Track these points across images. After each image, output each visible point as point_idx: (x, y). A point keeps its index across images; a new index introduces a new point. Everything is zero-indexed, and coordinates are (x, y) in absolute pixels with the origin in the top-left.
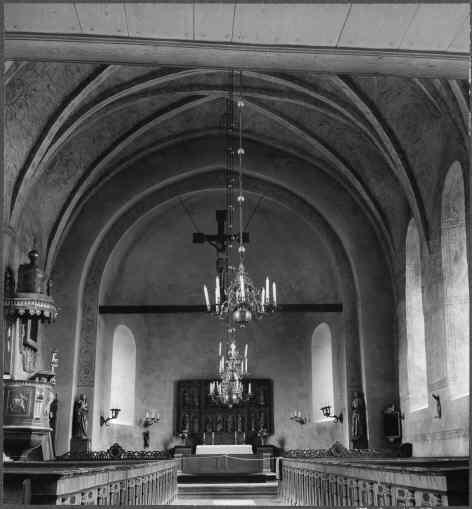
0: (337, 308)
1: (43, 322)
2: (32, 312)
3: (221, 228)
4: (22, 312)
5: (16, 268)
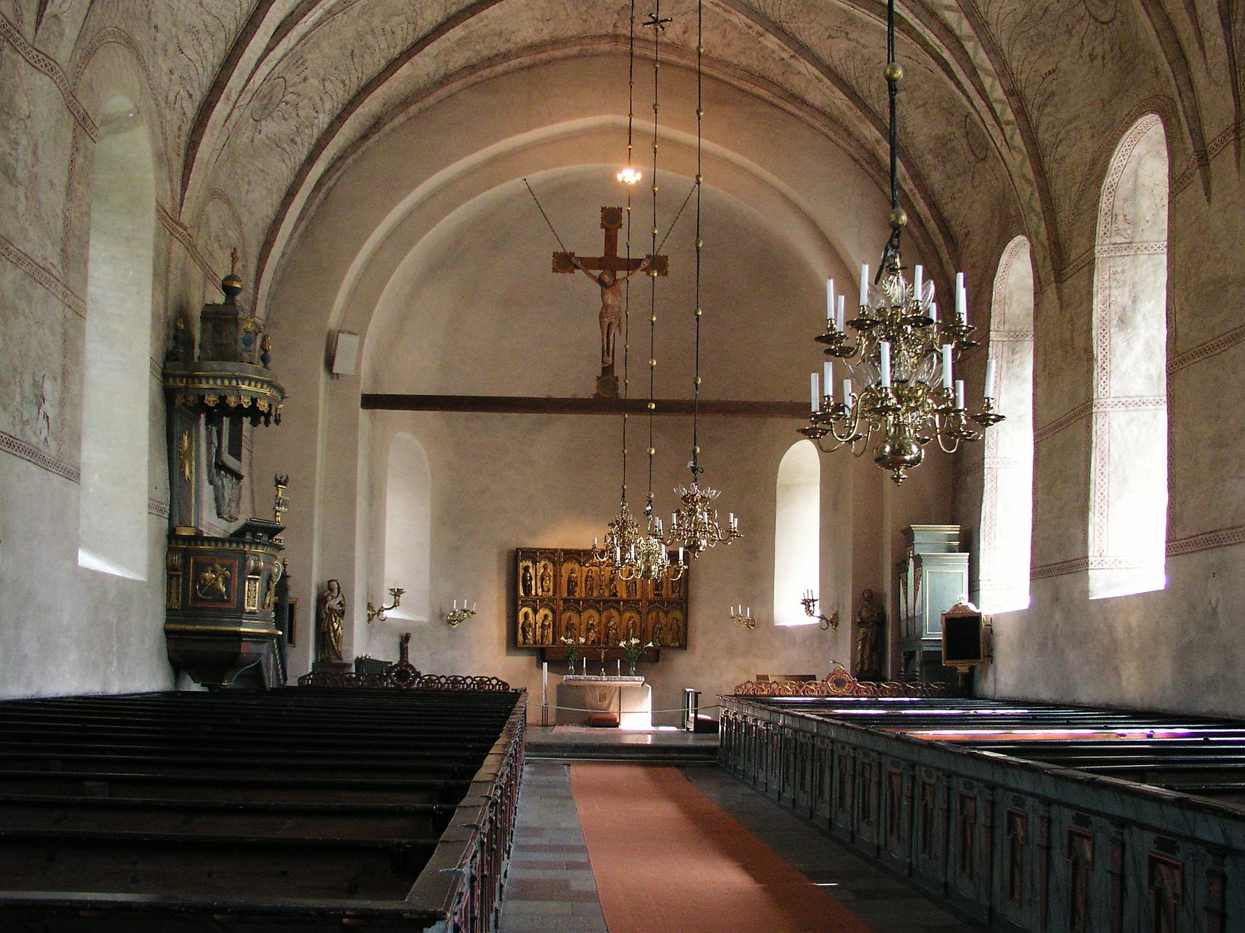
1: (255, 423)
2: (232, 401)
3: (611, 242)
4: (211, 400)
5: (197, 312)
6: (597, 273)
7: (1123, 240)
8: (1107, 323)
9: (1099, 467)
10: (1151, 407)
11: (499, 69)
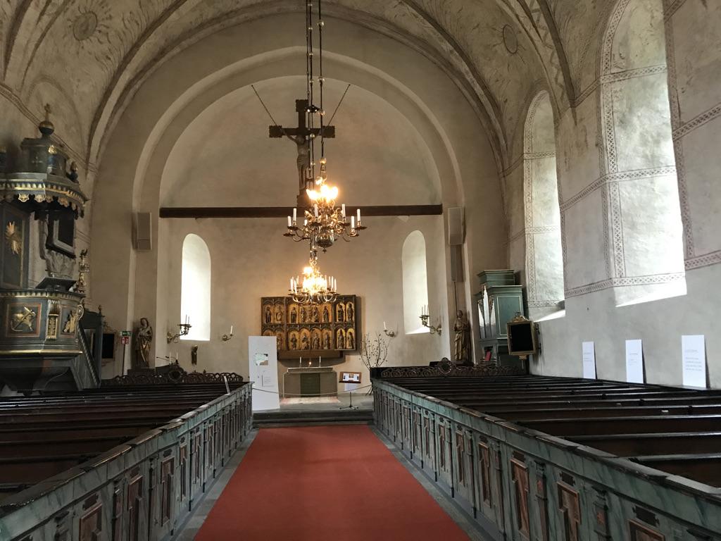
0: (435, 210)
3: (302, 119)
6: (294, 137)
7: (620, 70)
8: (612, 125)
9: (614, 218)
10: (648, 176)
11: (234, 20)
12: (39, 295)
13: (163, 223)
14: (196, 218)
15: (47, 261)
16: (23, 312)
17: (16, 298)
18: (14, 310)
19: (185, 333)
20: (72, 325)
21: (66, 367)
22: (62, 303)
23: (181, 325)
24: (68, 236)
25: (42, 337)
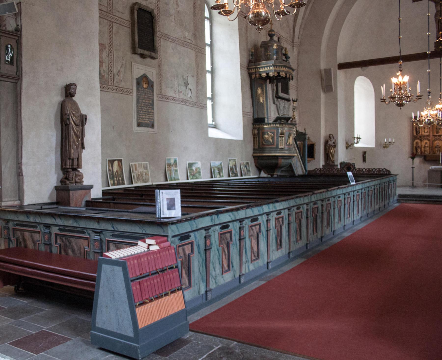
12: (274, 125)
13: (341, 74)
14: (361, 67)
15: (276, 105)
16: (268, 134)
17: (264, 128)
18: (264, 134)
19: (357, 143)
20: (291, 140)
21: (289, 163)
22: (286, 129)
23: (354, 138)
24: (286, 90)
25: (277, 147)
